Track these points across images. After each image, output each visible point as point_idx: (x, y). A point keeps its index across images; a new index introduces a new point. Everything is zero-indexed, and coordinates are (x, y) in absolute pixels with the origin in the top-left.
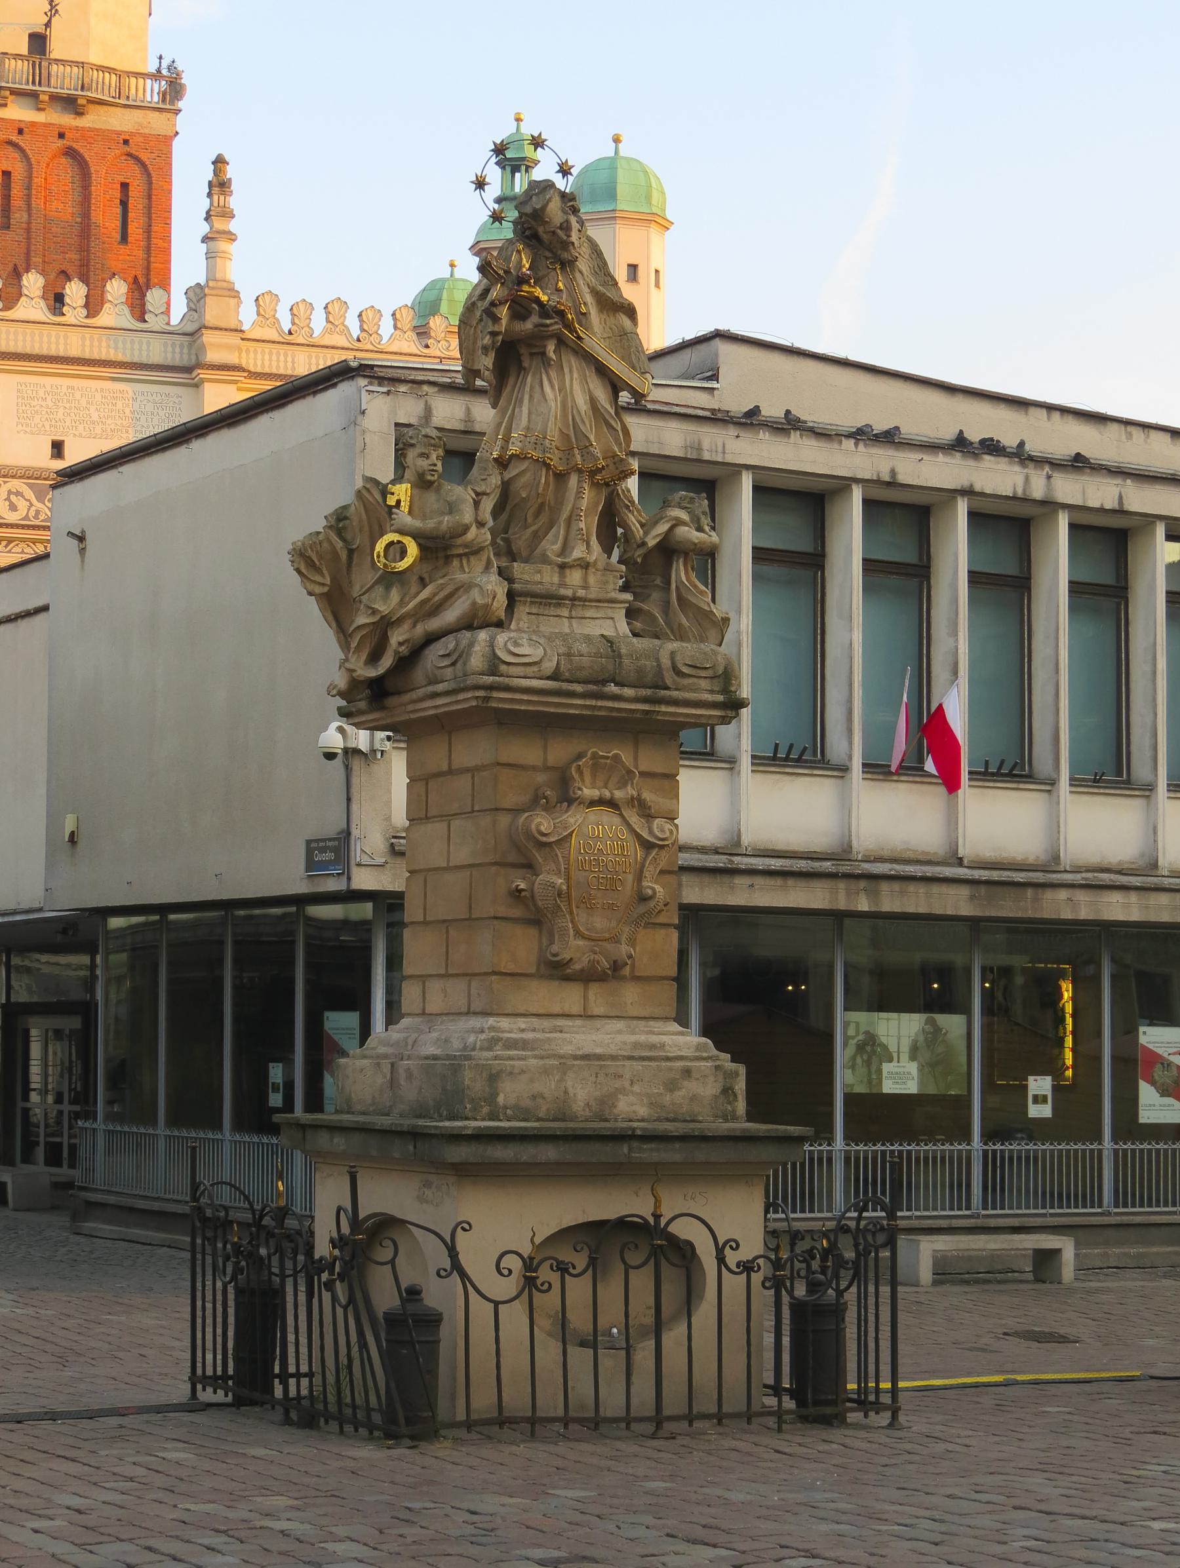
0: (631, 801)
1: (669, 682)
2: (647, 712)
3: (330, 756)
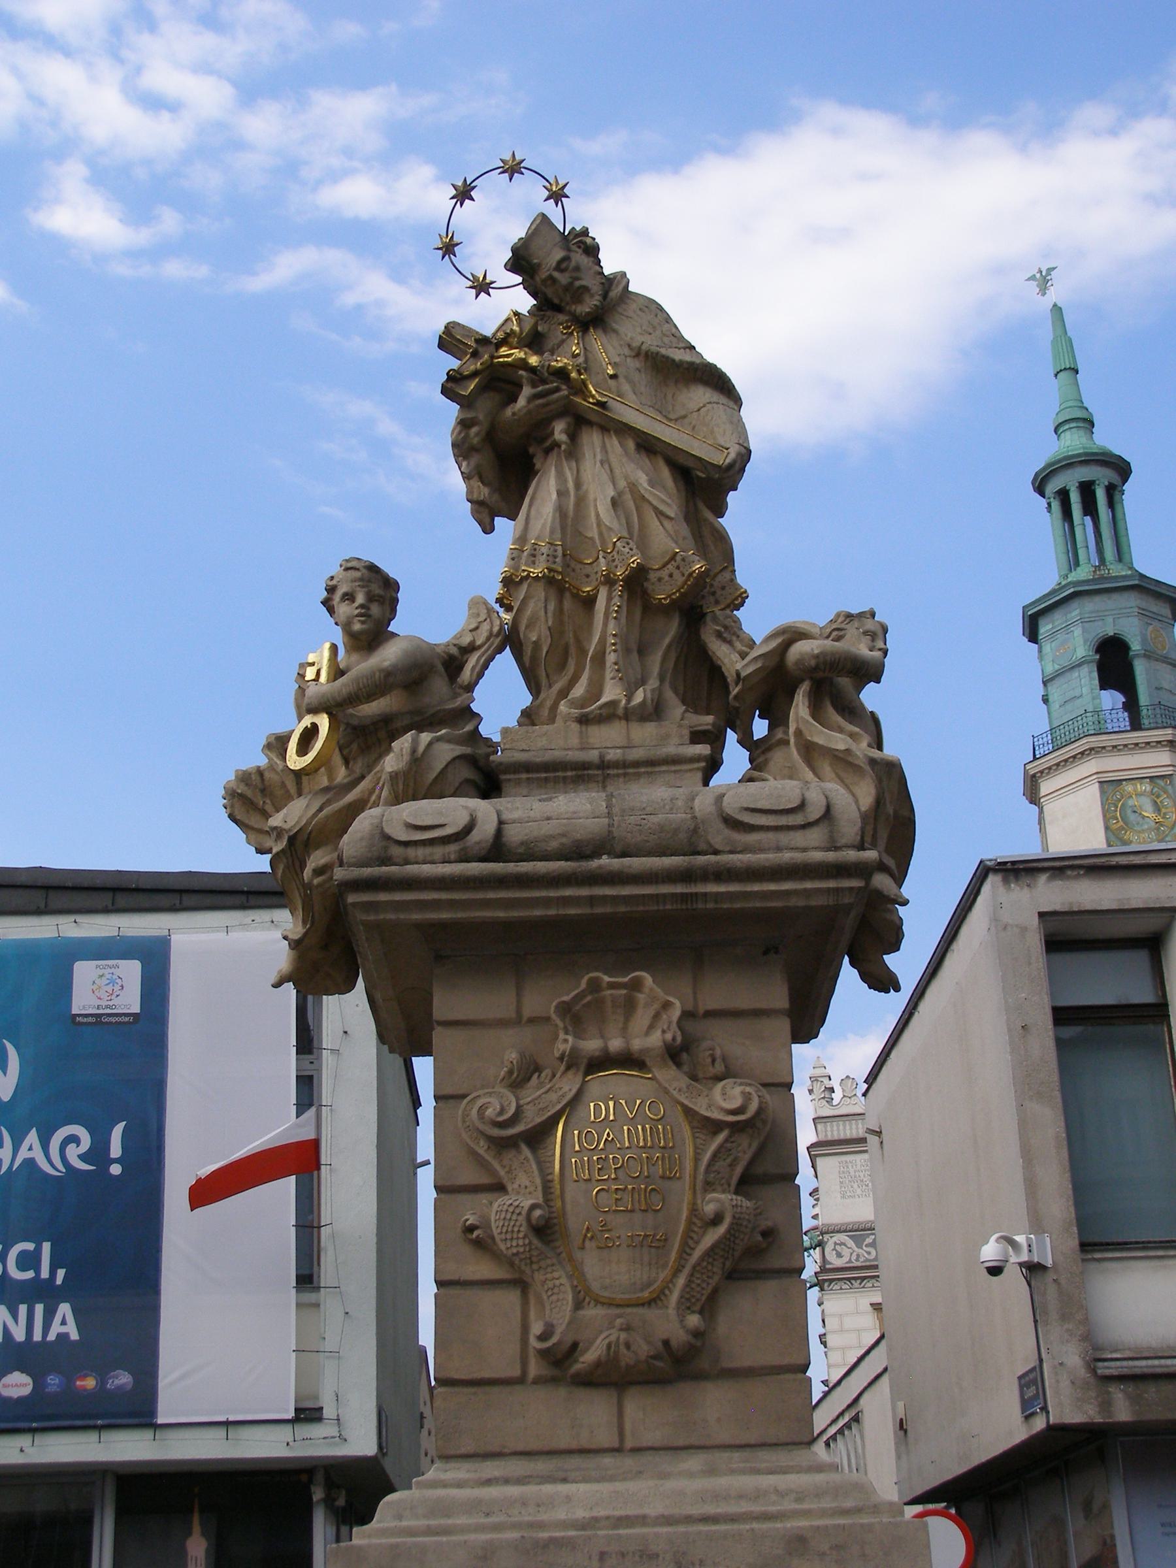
0: (675, 1054)
1: (717, 841)
2: (684, 897)
3: (995, 1271)
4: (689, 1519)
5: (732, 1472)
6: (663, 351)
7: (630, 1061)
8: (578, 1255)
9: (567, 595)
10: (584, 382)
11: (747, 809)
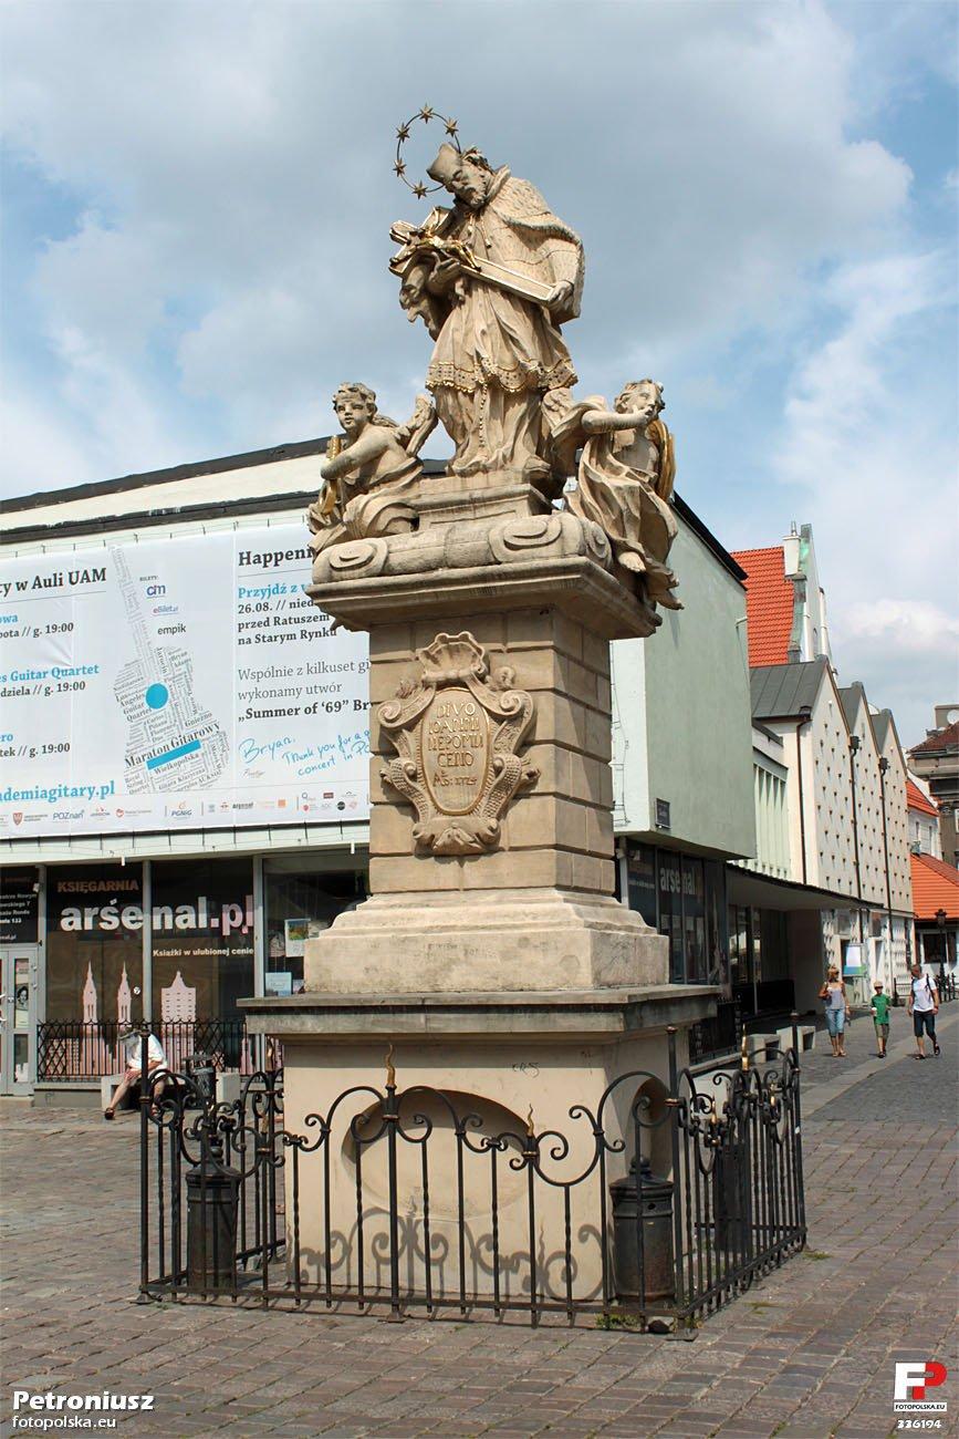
4: (477, 928)
5: (510, 902)
6: (524, 222)
7: (459, 683)
8: (432, 788)
9: (460, 394)
10: (468, 256)
11: (519, 537)
